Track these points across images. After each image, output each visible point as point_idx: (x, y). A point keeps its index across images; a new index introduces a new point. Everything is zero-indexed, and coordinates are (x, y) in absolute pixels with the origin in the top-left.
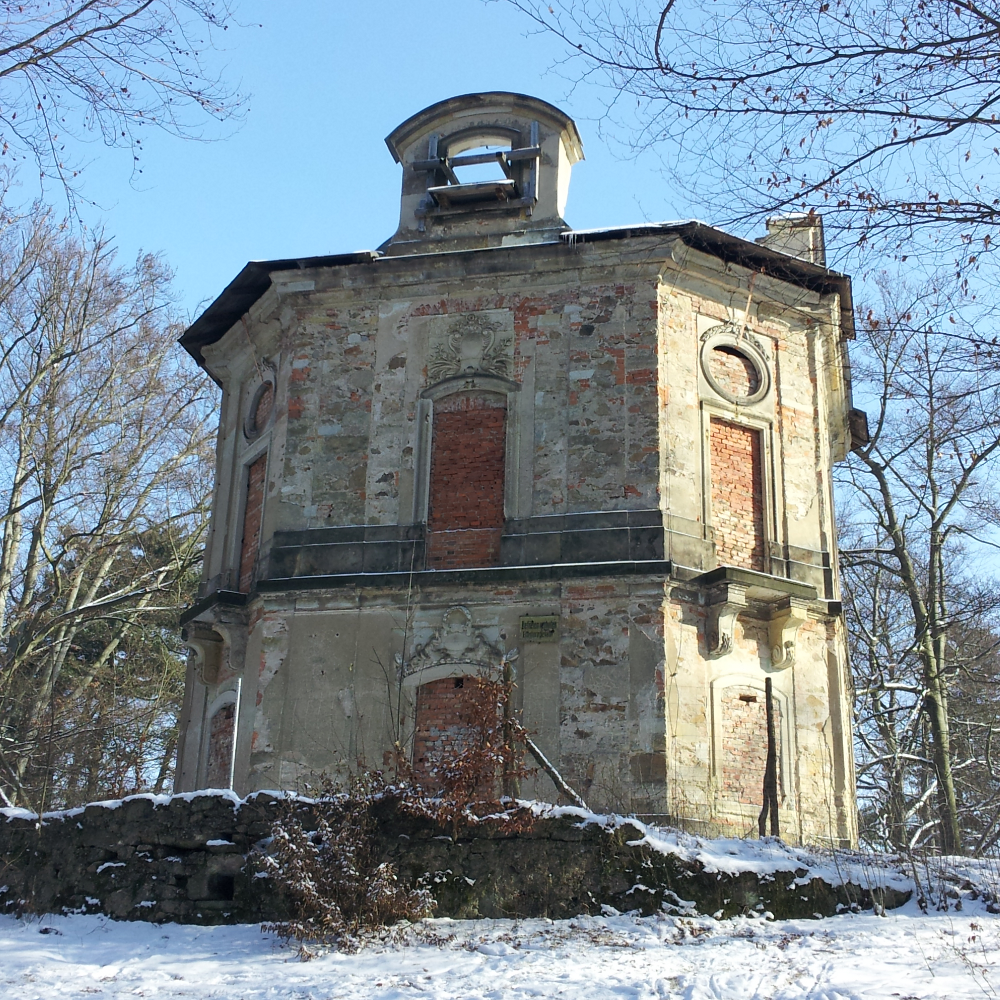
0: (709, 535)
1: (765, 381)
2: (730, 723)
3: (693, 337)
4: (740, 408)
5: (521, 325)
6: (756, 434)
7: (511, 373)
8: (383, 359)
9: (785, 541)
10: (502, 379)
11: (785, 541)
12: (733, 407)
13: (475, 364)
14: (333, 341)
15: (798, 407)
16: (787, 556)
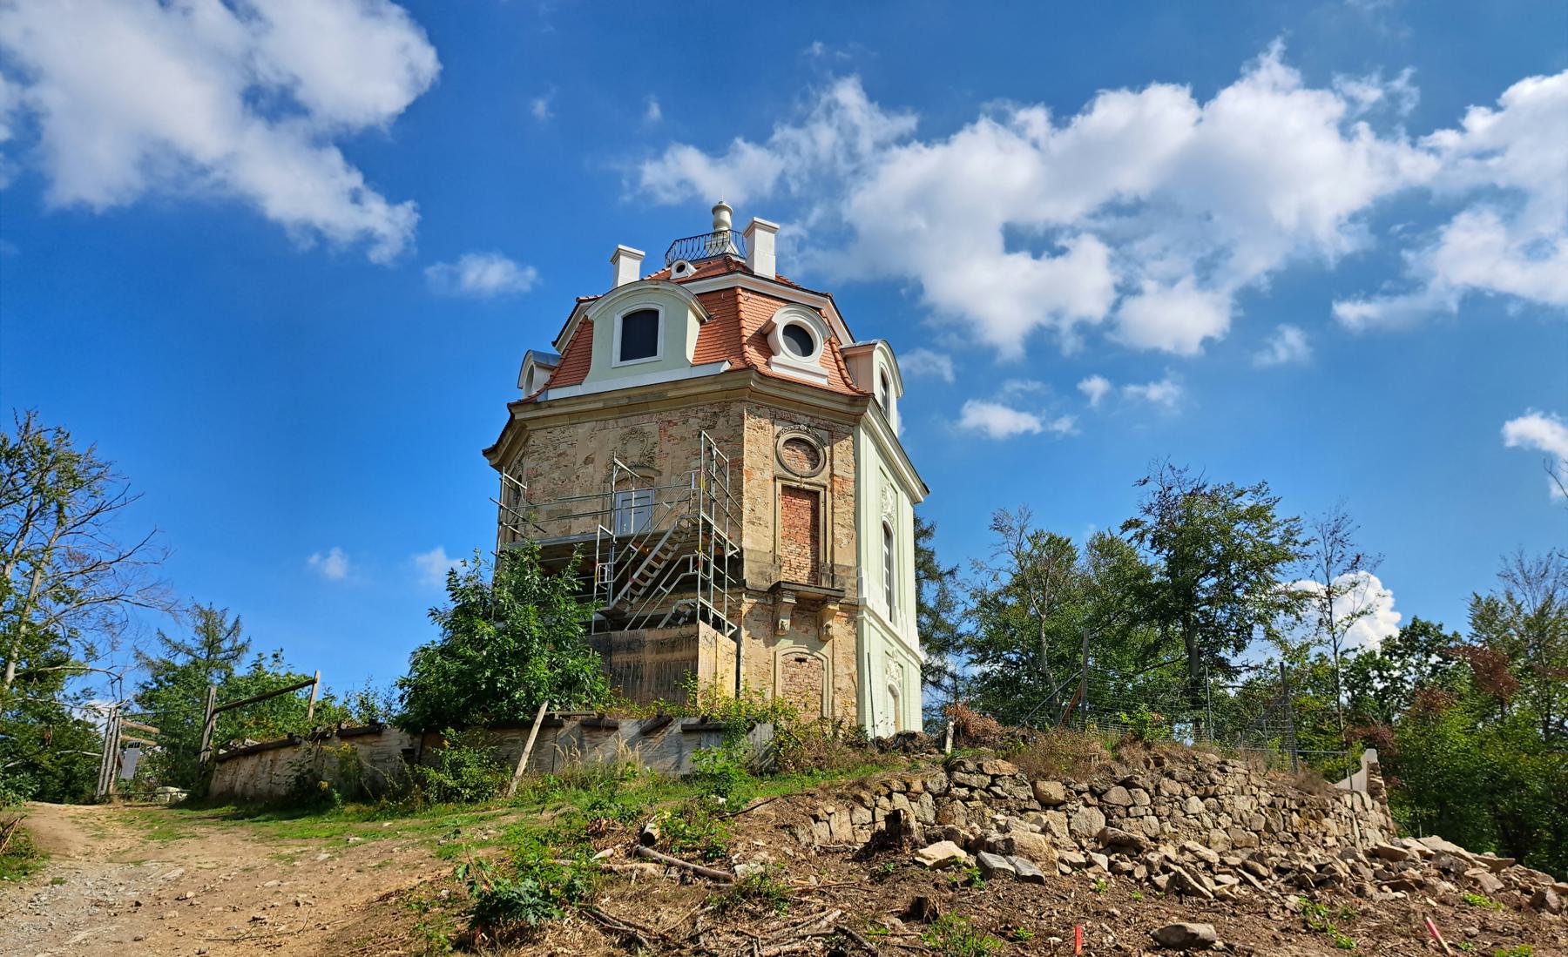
0: (778, 561)
1: (822, 459)
3: (771, 435)
4: (804, 480)
5: (663, 430)
6: (814, 495)
7: (658, 463)
8: (581, 458)
9: (832, 561)
10: (652, 469)
11: (832, 561)
12: (798, 479)
13: (636, 460)
14: (551, 448)
15: (845, 475)
16: (832, 571)
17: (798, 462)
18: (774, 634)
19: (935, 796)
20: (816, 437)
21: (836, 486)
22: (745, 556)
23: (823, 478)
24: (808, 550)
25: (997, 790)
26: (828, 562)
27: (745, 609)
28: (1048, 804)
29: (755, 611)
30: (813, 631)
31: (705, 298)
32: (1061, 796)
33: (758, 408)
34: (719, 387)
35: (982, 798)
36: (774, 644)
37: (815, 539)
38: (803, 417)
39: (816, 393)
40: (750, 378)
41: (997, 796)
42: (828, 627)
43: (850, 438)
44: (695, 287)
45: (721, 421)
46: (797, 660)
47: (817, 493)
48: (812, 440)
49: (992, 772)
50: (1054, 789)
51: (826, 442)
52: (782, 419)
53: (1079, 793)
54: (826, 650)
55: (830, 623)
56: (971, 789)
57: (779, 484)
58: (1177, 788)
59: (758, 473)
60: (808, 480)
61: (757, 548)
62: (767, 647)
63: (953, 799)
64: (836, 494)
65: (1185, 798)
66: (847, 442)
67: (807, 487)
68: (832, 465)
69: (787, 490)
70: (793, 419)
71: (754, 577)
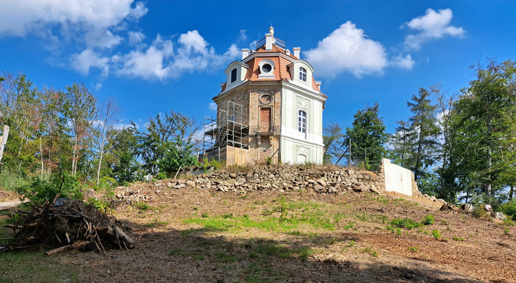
0: (259, 127)
9: (274, 125)
11: (274, 125)
12: (265, 105)
15: (278, 102)
16: (274, 127)
17: (264, 101)
21: (276, 105)
23: (272, 104)
24: (268, 123)
25: (221, 176)
26: (273, 125)
27: (250, 140)
30: (268, 144)
31: (248, 63)
32: (235, 176)
33: (254, 90)
34: (244, 86)
35: (218, 177)
37: (270, 120)
38: (266, 89)
39: (269, 82)
40: (249, 83)
41: (221, 177)
42: (271, 142)
43: (280, 91)
44: (245, 61)
45: (246, 95)
46: (264, 151)
47: (271, 108)
50: (234, 175)
51: (273, 94)
52: (261, 91)
53: (239, 175)
54: (271, 148)
57: (260, 108)
58: (267, 173)
59: (254, 106)
65: (269, 175)
66: (279, 93)
67: (268, 107)
69: (262, 109)
71: (252, 132)
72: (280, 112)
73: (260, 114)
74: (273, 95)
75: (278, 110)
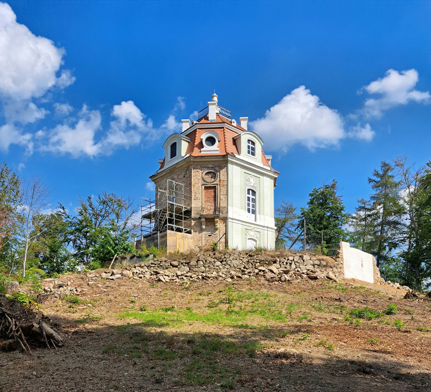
0: (203, 209)
1: (217, 176)
2: (206, 240)
6: (214, 188)
11: (220, 206)
12: (209, 184)
15: (224, 179)
16: (219, 209)
17: (208, 178)
18: (201, 230)
19: (147, 267)
20: (215, 170)
21: (221, 183)
22: (193, 209)
24: (213, 204)
25: (161, 264)
26: (219, 206)
27: (193, 224)
28: (174, 266)
29: (196, 224)
30: (213, 227)
31: (189, 135)
32: (177, 264)
33: (196, 166)
35: (157, 266)
36: (202, 232)
37: (215, 200)
40: (191, 159)
41: (161, 266)
42: (216, 225)
43: (226, 168)
46: (209, 236)
47: (216, 187)
48: (212, 171)
49: (160, 260)
50: (175, 263)
51: (218, 171)
53: (182, 263)
55: (217, 224)
56: (155, 265)
57: (203, 187)
59: (197, 185)
60: (212, 184)
61: (196, 206)
62: (199, 234)
63: (151, 267)
64: (221, 186)
66: (224, 170)
68: (220, 177)
69: (206, 188)
70: (208, 167)
72: (226, 191)
73: (203, 193)
74: (218, 172)
75: (224, 189)
